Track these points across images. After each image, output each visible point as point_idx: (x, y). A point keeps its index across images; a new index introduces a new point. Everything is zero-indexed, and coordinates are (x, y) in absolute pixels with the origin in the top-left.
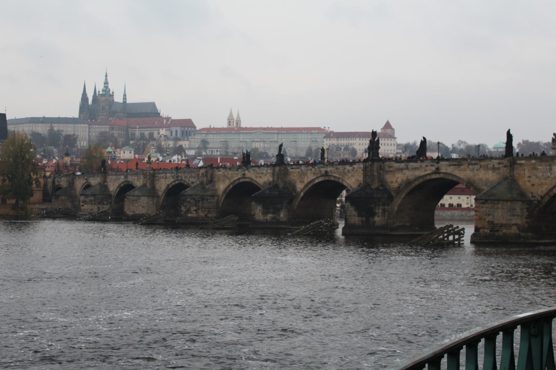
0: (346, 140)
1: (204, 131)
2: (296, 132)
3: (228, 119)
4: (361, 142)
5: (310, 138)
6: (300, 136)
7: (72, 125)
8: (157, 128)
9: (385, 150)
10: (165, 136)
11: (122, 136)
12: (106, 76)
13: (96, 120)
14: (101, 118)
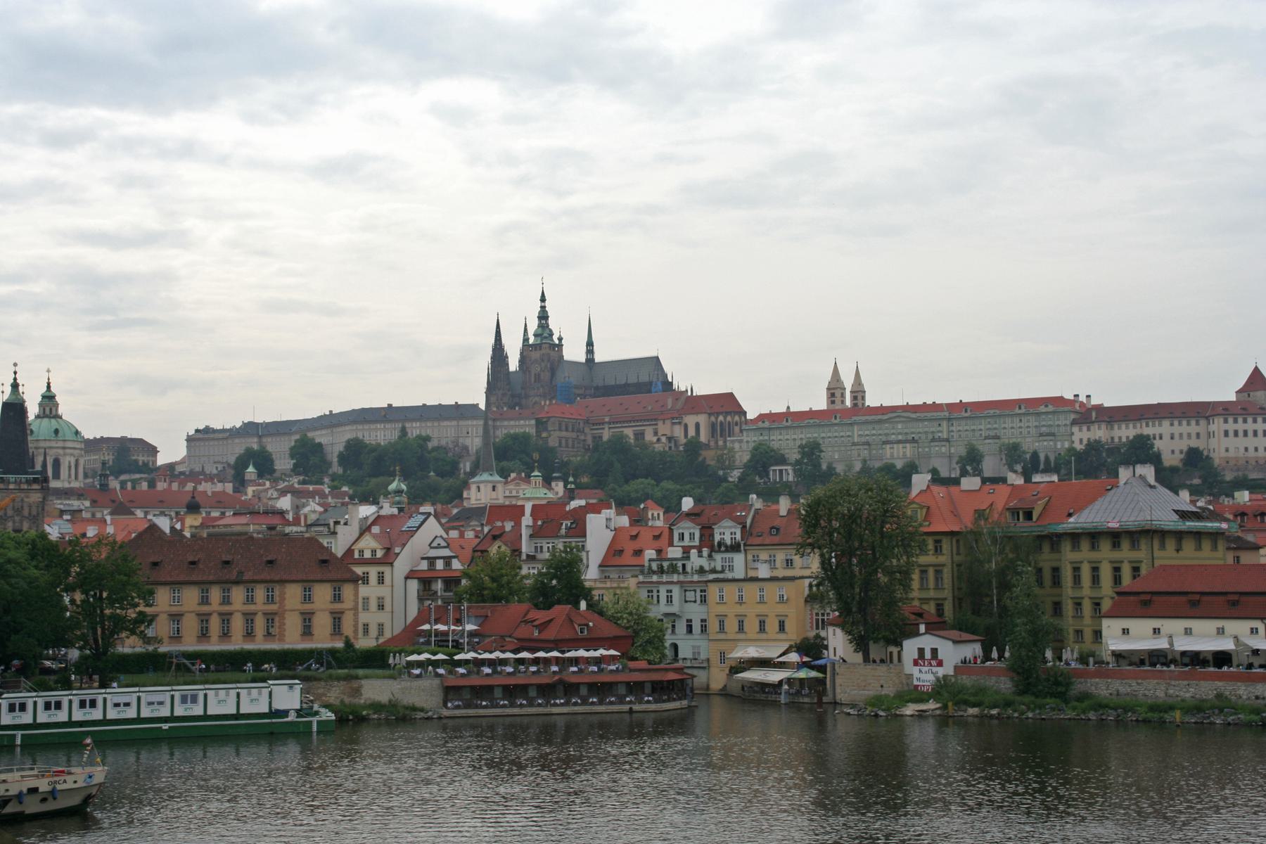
0: (1135, 427)
1: (763, 422)
2: (998, 412)
3: (828, 389)
4: (1177, 429)
5: (1036, 427)
6: (1008, 423)
7: (454, 423)
8: (652, 420)
9: (1246, 449)
10: (670, 439)
11: (570, 442)
12: (543, 299)
13: (521, 407)
14: (534, 401)
